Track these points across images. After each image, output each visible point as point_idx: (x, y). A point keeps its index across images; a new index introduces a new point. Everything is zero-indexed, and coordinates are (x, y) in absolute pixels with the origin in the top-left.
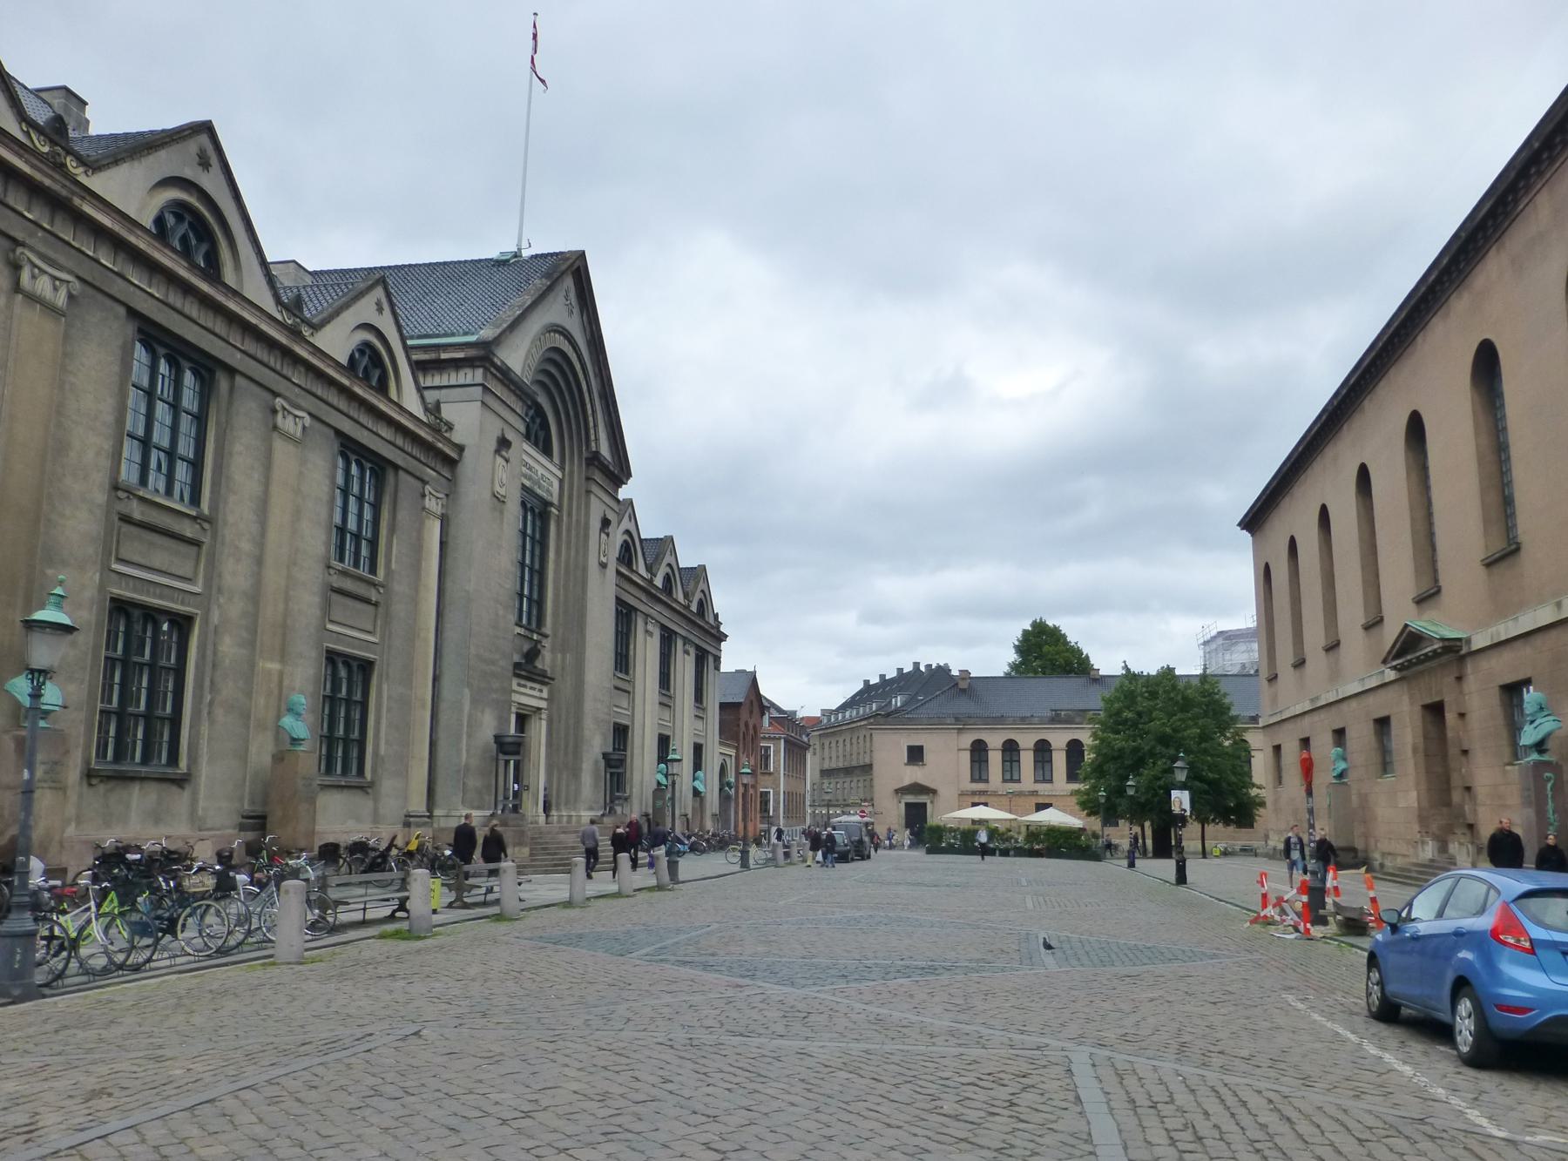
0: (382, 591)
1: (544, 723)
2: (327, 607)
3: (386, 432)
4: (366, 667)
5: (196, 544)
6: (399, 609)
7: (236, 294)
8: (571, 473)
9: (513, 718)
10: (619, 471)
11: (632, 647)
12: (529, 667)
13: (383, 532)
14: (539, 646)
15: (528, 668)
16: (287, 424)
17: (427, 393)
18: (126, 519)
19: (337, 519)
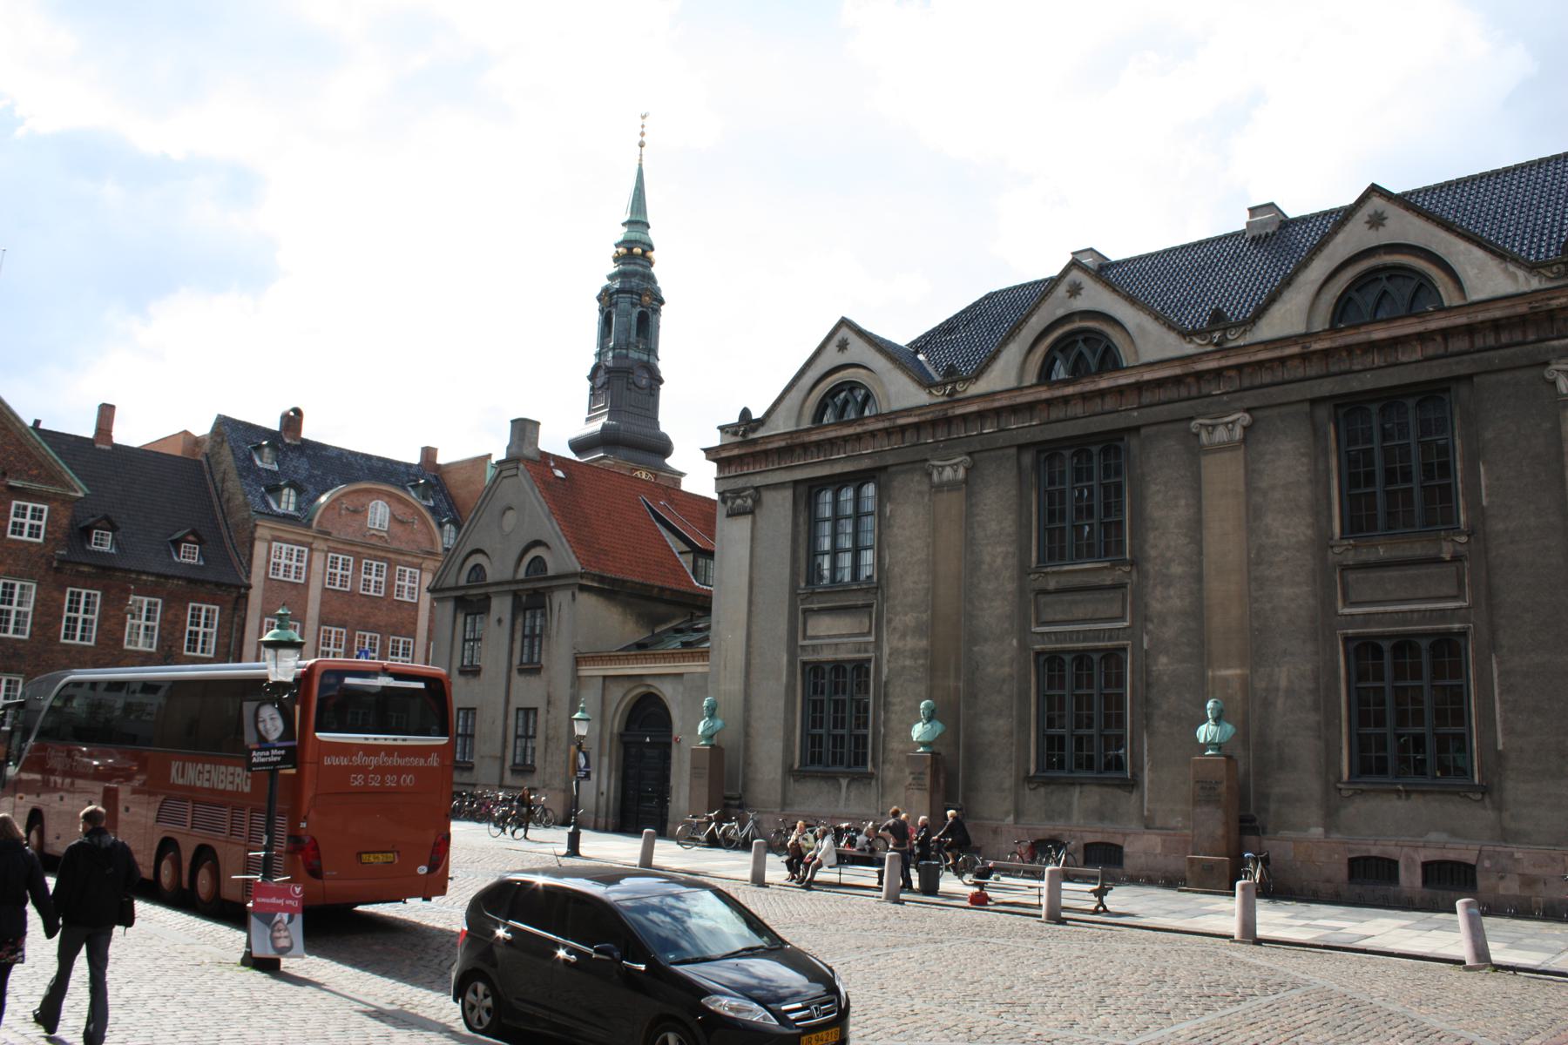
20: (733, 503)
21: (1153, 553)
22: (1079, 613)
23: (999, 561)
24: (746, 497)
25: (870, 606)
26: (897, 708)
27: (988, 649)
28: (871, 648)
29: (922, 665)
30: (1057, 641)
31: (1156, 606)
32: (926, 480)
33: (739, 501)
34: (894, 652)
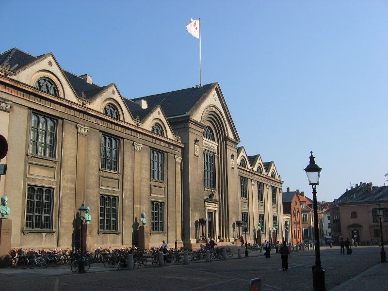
2: (151, 190)
4: (162, 204)
9: (206, 214)
16: (137, 148)
18: (102, 177)
23: (94, 164)
26: (65, 207)
27: (91, 191)
28: (55, 183)
34: (64, 187)
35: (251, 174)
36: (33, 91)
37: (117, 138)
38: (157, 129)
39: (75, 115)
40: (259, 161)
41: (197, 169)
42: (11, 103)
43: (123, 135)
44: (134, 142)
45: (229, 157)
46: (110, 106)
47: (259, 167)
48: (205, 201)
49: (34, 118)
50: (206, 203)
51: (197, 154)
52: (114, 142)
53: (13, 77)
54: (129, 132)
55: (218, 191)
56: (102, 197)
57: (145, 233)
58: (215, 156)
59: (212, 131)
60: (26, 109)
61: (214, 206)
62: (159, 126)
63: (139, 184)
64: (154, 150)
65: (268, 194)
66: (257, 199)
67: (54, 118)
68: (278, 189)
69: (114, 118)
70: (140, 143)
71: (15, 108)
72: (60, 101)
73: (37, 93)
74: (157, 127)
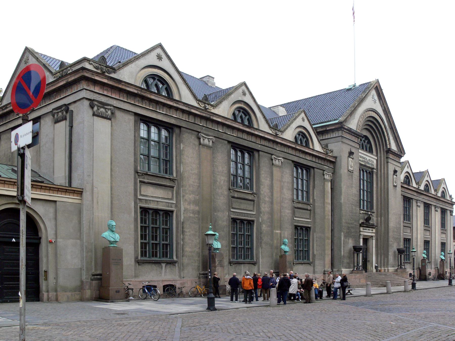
0: (311, 206)
1: (374, 241)
2: (294, 213)
3: (309, 158)
4: (308, 229)
5: (253, 201)
6: (318, 210)
7: (257, 129)
8: (381, 157)
10: (401, 152)
11: (411, 212)
12: (367, 223)
13: (311, 188)
14: (371, 216)
15: (367, 223)
16: (276, 162)
17: (322, 142)
18: (233, 197)
19: (295, 186)
20: (98, 109)
21: (262, 192)
22: (242, 206)
23: (222, 182)
24: (108, 109)
25: (173, 187)
26: (188, 234)
28: (173, 206)
29: (197, 217)
30: (237, 215)
31: (263, 209)
32: (197, 140)
33: (102, 110)
34: (186, 210)
35: (415, 194)
36: (139, 92)
37: (251, 151)
38: (301, 140)
39: (196, 122)
40: (426, 178)
41: (352, 187)
42: (112, 108)
43: (259, 147)
44: (272, 155)
45: (391, 172)
46: (239, 111)
47: (426, 186)
48: (361, 225)
49: (143, 127)
50: (361, 229)
51: (352, 169)
52: (246, 155)
53: (113, 75)
54: (263, 142)
55: (375, 213)
56: (234, 220)
57: (287, 263)
58: (373, 172)
59: (369, 142)
60: (132, 115)
61: (371, 231)
62: (304, 135)
63: (279, 205)
64: (297, 165)
65: (436, 217)
66: (423, 223)
67: (169, 127)
68: (448, 212)
69: (246, 125)
70: (280, 157)
71: (118, 114)
72: (175, 105)
73: (144, 94)
74: (301, 137)
